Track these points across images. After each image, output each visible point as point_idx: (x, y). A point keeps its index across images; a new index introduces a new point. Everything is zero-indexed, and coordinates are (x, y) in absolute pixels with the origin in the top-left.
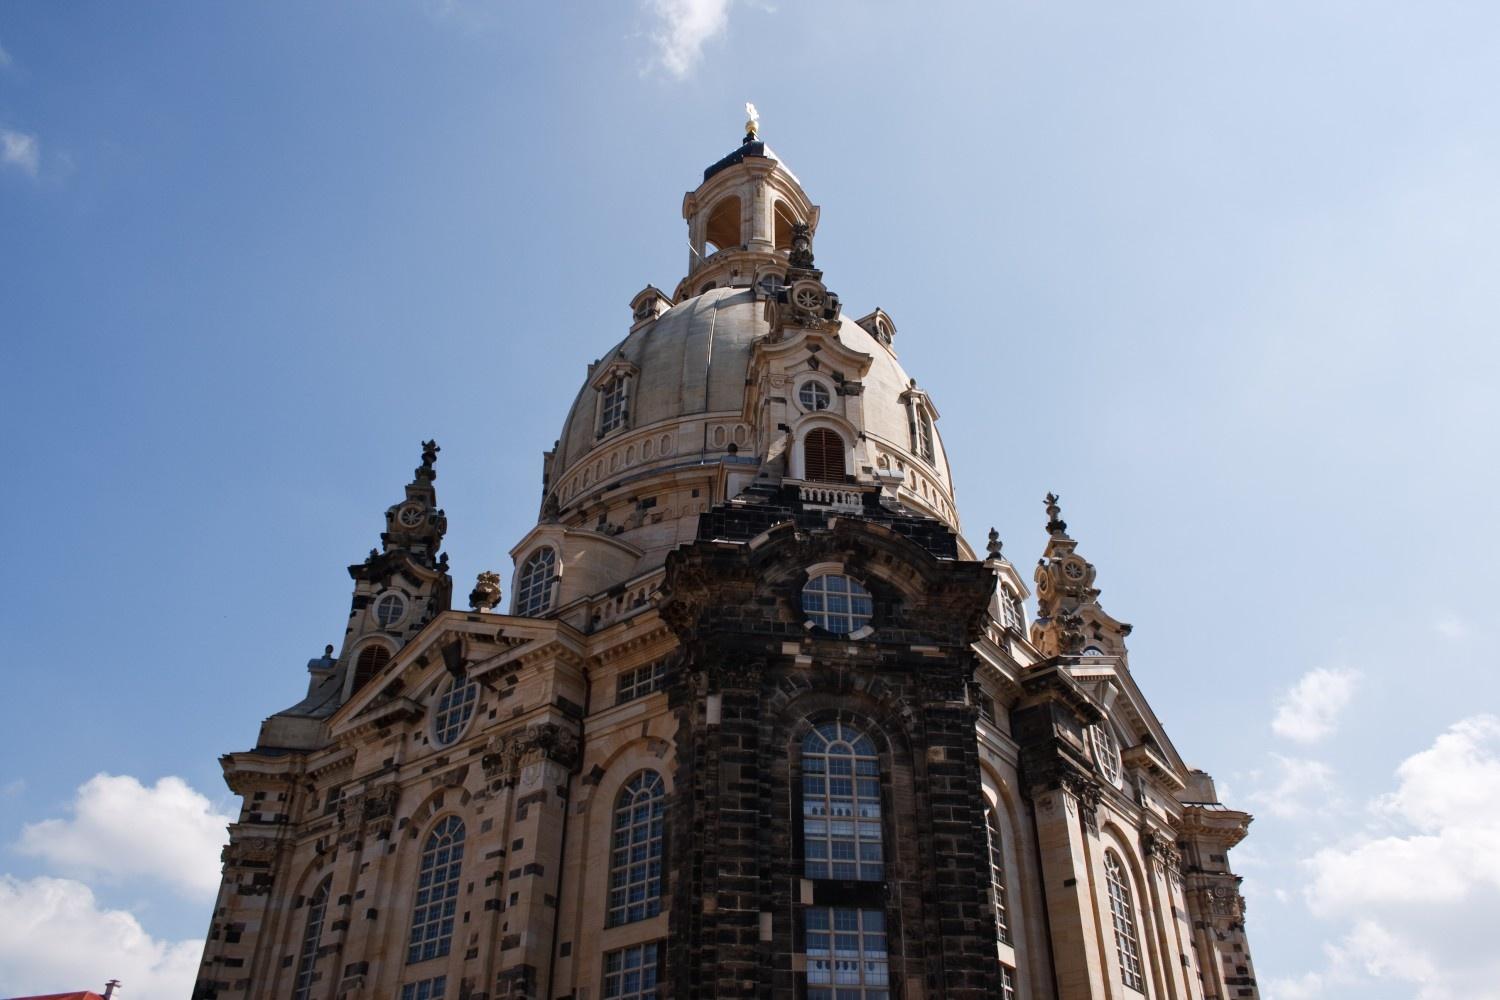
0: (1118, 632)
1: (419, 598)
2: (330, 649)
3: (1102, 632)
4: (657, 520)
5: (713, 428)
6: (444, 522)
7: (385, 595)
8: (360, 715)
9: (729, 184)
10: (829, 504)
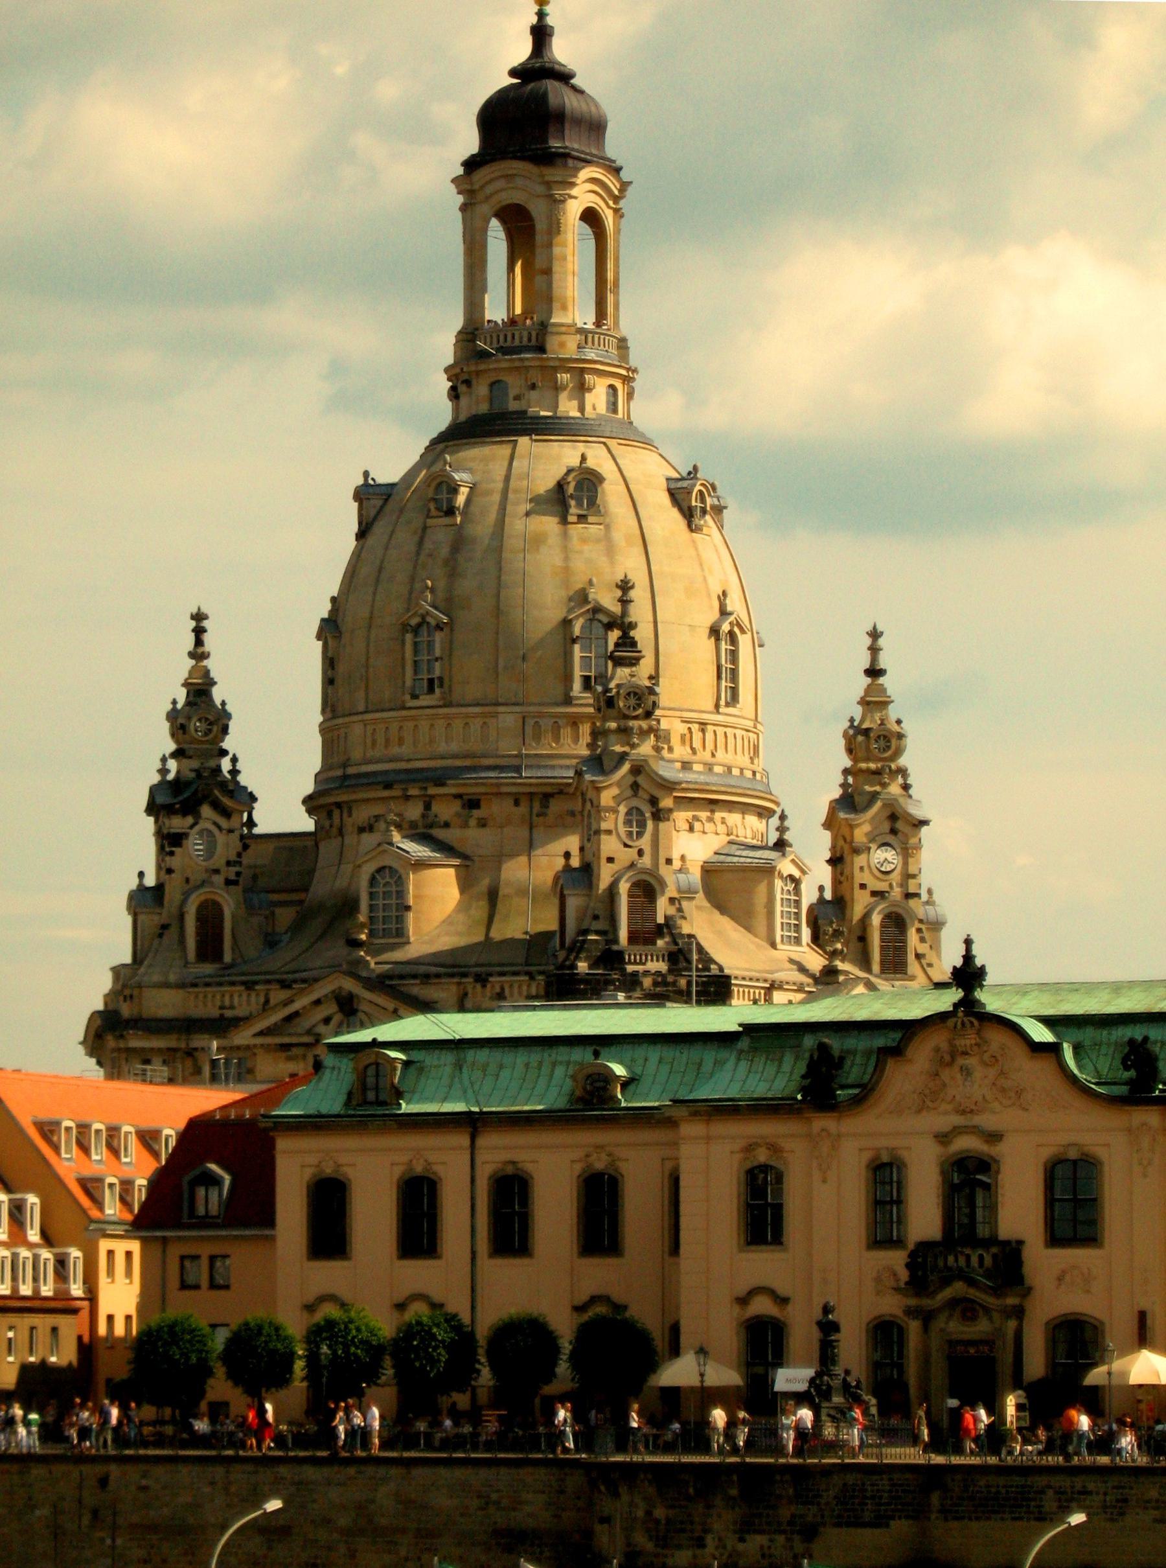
0: (914, 825)
1: (230, 831)
2: (141, 875)
3: (899, 825)
4: (482, 823)
5: (530, 722)
6: (228, 716)
7: (197, 828)
8: (261, 1033)
9: (519, 182)
10: (644, 964)
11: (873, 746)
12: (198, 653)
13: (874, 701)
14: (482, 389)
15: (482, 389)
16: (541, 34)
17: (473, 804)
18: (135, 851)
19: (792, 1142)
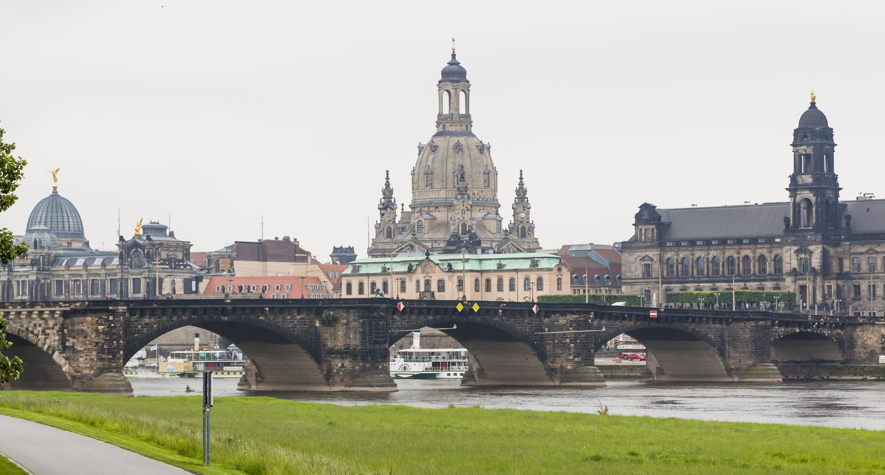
11: (521, 193)
12: (387, 179)
13: (521, 184)
14: (441, 126)
15: (441, 126)
16: (454, 56)
17: (437, 207)
18: (376, 217)
19: (407, 277)
